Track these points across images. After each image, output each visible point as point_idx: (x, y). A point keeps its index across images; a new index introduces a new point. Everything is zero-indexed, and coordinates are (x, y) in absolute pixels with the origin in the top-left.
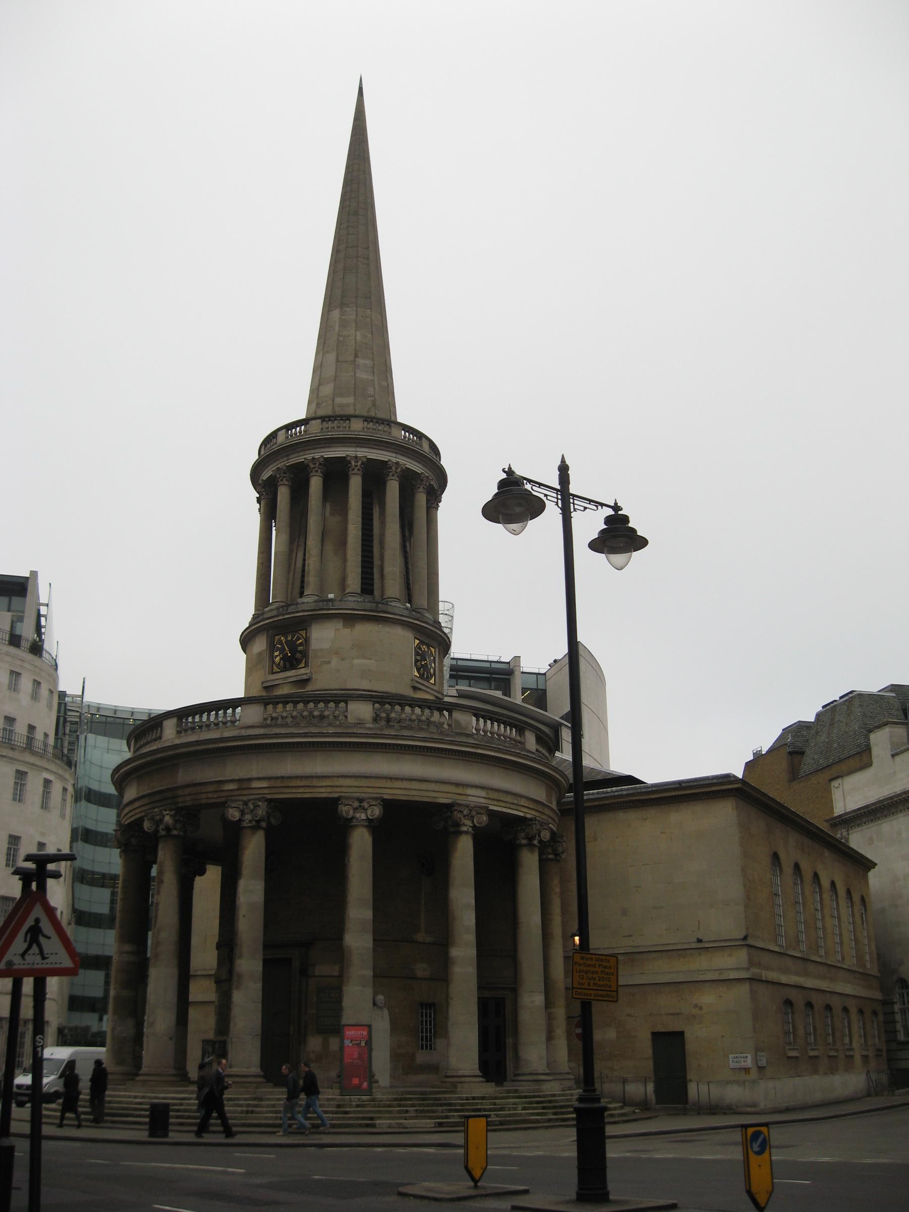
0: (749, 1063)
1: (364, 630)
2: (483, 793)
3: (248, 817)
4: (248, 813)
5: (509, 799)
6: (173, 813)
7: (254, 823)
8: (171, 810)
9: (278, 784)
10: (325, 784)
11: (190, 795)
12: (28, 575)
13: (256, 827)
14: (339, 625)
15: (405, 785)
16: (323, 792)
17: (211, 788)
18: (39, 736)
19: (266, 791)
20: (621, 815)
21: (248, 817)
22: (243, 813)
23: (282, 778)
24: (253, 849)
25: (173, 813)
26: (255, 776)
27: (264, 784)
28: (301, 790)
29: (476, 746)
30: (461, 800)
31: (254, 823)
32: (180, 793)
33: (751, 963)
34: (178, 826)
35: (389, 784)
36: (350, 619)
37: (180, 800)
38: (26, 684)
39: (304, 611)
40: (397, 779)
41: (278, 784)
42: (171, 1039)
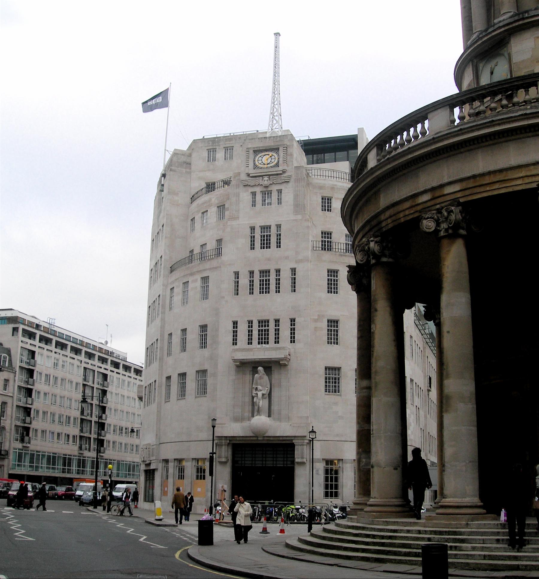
3: (444, 226)
4: (443, 222)
6: (378, 239)
7: (450, 231)
8: (376, 237)
9: (471, 184)
10: (521, 175)
11: (390, 217)
12: (357, 134)
13: (453, 236)
17: (407, 205)
19: (459, 195)
21: (444, 226)
22: (438, 224)
23: (474, 177)
24: (454, 260)
25: (378, 239)
26: (446, 180)
27: (456, 187)
28: (497, 186)
31: (450, 231)
32: (382, 217)
34: (387, 252)
37: (384, 224)
39: (500, 28)
41: (471, 184)
42: (395, 469)
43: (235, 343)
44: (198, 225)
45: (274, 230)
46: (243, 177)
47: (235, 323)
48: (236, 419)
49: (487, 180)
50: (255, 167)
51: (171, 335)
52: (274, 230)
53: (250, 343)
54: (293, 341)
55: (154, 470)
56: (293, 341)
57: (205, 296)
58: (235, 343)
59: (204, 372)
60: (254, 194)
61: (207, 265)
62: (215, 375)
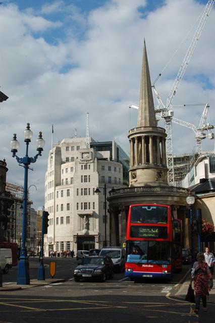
14: (141, 170)
18: (118, 180)
38: (112, 169)
43: (78, 209)
45: (88, 177)
51: (57, 205)
52: (88, 177)
53: (82, 209)
54: (94, 208)
55: (53, 245)
56: (94, 208)
58: (78, 209)
59: (69, 217)
60: (82, 166)
61: (69, 186)
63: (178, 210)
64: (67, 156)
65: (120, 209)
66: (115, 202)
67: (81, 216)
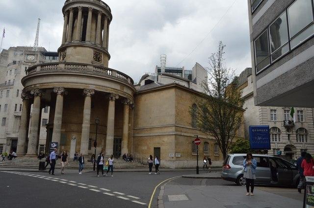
0: (173, 156)
1: (78, 49)
2: (94, 86)
5: (101, 87)
13: (37, 95)
14: (72, 48)
15: (71, 84)
16: (51, 87)
20: (151, 94)
29: (91, 74)
30: (87, 88)
33: (176, 130)
35: (67, 84)
36: (75, 46)
40: (69, 83)
43: (15, 110)
44: (8, 74)
46: (23, 62)
47: (16, 105)
48: (14, 132)
49: (45, 84)
50: (27, 59)
57: (7, 96)
58: (15, 110)
62: (8, 119)
63: (116, 101)
64: (15, 59)
65: (32, 93)
66: (29, 84)
67: (16, 117)
